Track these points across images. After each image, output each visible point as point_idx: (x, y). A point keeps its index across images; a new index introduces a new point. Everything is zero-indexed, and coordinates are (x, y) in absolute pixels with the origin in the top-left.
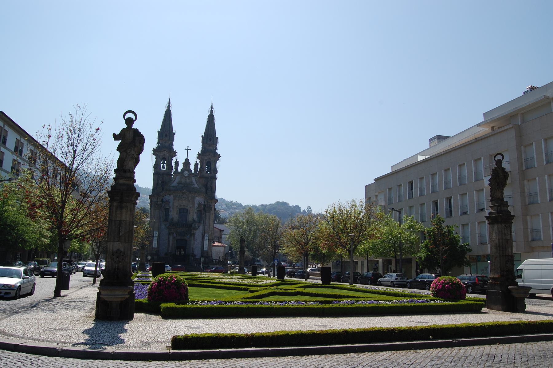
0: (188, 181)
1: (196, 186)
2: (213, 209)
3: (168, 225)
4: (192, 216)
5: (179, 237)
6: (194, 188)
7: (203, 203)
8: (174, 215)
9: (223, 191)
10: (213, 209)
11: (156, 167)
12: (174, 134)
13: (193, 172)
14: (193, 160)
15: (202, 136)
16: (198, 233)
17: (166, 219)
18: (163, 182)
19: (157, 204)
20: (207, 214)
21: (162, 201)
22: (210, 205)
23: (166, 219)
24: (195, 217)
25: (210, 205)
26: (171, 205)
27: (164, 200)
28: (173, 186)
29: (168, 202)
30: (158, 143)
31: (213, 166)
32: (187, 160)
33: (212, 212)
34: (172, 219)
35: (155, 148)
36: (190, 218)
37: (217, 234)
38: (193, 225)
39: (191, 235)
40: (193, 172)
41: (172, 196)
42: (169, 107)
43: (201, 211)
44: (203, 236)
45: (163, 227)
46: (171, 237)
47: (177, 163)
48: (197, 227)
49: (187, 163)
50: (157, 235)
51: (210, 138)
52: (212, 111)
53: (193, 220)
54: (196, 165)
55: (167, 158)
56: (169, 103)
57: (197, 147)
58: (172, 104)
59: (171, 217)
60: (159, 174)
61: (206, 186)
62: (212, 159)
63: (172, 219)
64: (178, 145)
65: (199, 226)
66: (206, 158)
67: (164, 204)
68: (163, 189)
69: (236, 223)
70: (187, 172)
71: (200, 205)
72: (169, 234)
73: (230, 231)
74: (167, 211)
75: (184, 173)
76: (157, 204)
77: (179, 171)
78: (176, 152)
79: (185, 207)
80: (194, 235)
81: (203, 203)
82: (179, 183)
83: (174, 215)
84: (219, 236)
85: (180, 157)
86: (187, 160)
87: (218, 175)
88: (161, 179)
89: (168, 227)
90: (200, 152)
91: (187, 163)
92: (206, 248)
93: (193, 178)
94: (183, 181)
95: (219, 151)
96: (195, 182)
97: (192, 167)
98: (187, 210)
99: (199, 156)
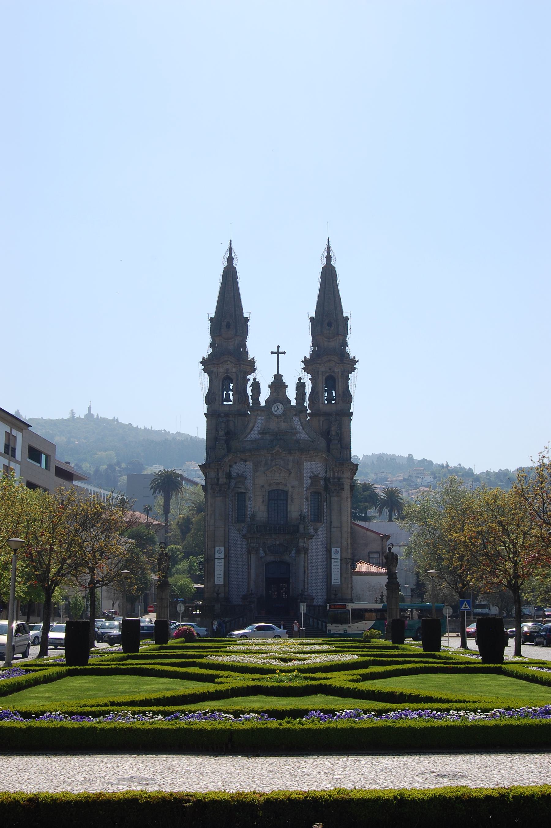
0: (283, 426)
1: (303, 436)
2: (347, 487)
3: (244, 532)
4: (299, 506)
5: (270, 558)
6: (297, 441)
7: (323, 475)
8: (257, 506)
9: (364, 442)
10: (347, 487)
11: (210, 399)
12: (247, 320)
13: (293, 403)
14: (294, 373)
15: (311, 319)
16: (316, 547)
17: (240, 519)
18: (228, 433)
19: (217, 484)
20: (335, 499)
21: (229, 476)
22: (339, 479)
24: (306, 509)
25: (339, 479)
26: (249, 483)
27: (234, 474)
29: (242, 478)
30: (212, 345)
31: (340, 385)
32: (278, 377)
33: (346, 493)
34: (254, 516)
35: (206, 356)
36: (294, 511)
37: (375, 546)
38: (301, 527)
39: (298, 552)
40: (293, 403)
41: (250, 464)
43: (319, 493)
44: (328, 552)
45: (235, 535)
46: (253, 558)
47: (256, 386)
48: (312, 532)
49: (278, 384)
50: (222, 555)
51: (329, 322)
52: (329, 258)
53: (302, 517)
54: (300, 386)
55: (234, 377)
56: (231, 250)
57: (302, 345)
58: (237, 254)
59: (249, 513)
60: (219, 416)
61: (326, 434)
62: (338, 369)
63: (254, 516)
64: (257, 346)
65: (316, 530)
66: (322, 369)
67: (233, 482)
68: (229, 450)
69: (423, 515)
70: (281, 406)
71: (314, 479)
72: (249, 552)
73: (412, 538)
74: (241, 497)
75: (274, 408)
76: (217, 484)
77: (263, 404)
78: (253, 361)
79: (281, 487)
80: (306, 550)
81: (323, 475)
82: (263, 432)
83: (257, 506)
84: (379, 549)
85: (264, 376)
86: (278, 377)
87: (354, 408)
88: (223, 426)
89: (244, 536)
90: (308, 357)
92: (336, 579)
93: (296, 420)
94: (273, 426)
95: (352, 350)
96: (299, 427)
97: (291, 394)
98: (286, 493)
99: (309, 365)
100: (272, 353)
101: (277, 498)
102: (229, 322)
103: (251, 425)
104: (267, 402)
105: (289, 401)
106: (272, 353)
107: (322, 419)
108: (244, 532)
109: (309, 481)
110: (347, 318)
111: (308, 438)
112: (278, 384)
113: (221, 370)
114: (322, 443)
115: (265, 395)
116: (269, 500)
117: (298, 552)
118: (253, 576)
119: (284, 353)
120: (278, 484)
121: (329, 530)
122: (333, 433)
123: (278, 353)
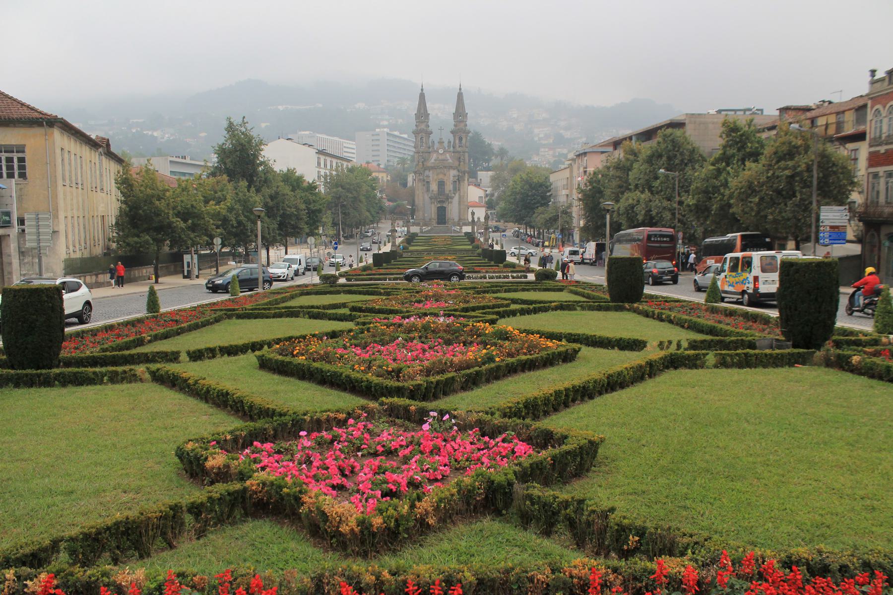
8: (434, 187)
14: (448, 137)
23: (428, 190)
24: (451, 187)
29: (428, 176)
32: (441, 139)
42: (422, 90)
54: (449, 142)
86: (441, 139)
91: (441, 142)
97: (446, 144)
101: (441, 184)
102: (422, 114)
112: (441, 142)
114: (457, 163)
115: (436, 145)
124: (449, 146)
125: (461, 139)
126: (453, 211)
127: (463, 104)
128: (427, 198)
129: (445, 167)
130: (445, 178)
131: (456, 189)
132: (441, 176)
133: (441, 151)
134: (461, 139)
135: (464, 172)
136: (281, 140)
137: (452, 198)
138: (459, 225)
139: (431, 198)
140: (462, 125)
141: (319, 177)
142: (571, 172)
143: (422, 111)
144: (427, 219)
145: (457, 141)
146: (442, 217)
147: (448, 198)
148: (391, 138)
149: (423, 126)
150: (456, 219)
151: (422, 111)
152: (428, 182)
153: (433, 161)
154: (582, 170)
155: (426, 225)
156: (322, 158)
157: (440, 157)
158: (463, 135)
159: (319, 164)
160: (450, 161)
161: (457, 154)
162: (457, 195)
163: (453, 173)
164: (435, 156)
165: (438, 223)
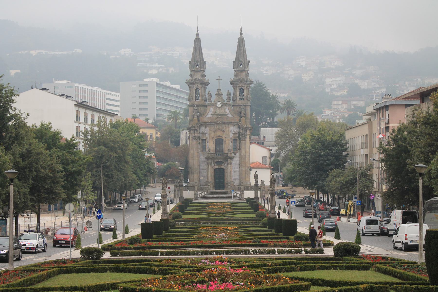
0: (221, 111)
1: (230, 116)
4: (228, 146)
8: (211, 146)
12: (205, 62)
13: (226, 102)
15: (234, 62)
20: (243, 142)
24: (231, 146)
26: (207, 136)
28: (208, 118)
29: (204, 133)
32: (219, 90)
38: (229, 155)
39: (228, 165)
40: (226, 102)
42: (198, 34)
43: (236, 139)
54: (229, 94)
59: (207, 148)
72: (208, 164)
80: (231, 164)
86: (219, 90)
89: (206, 158)
91: (219, 95)
96: (228, 112)
97: (225, 97)
98: (223, 139)
100: (217, 79)
101: (219, 142)
102: (198, 62)
103: (208, 111)
104: (214, 101)
105: (224, 101)
106: (217, 79)
107: (238, 107)
108: (206, 156)
109: (232, 135)
110: (249, 61)
111: (231, 116)
113: (195, 86)
114: (237, 119)
115: (214, 98)
116: (216, 143)
117: (228, 165)
118: (209, 175)
119: (222, 80)
120: (219, 136)
121: (240, 155)
122: (242, 114)
123: (219, 80)
124: (228, 99)
125: (242, 91)
126: (233, 173)
127: (244, 52)
128: (202, 157)
129: (224, 123)
130: (224, 136)
131: (237, 148)
132: (219, 133)
133: (219, 105)
134: (242, 91)
135: (246, 129)
136: (34, 89)
137: (232, 158)
138: (239, 189)
139: (207, 159)
140: (243, 75)
141: (78, 134)
142: (371, 128)
143: (198, 59)
144: (203, 184)
145: (238, 93)
146: (220, 180)
147: (227, 159)
148: (161, 89)
149: (198, 76)
150: (237, 183)
151: (198, 59)
152: (203, 140)
153: (209, 115)
154: (383, 125)
155: (201, 189)
156: (82, 111)
157: (218, 112)
158: (245, 86)
159: (78, 118)
160: (230, 116)
161: (237, 109)
162: (238, 154)
163: (233, 130)
164: (211, 110)
165: (216, 187)
